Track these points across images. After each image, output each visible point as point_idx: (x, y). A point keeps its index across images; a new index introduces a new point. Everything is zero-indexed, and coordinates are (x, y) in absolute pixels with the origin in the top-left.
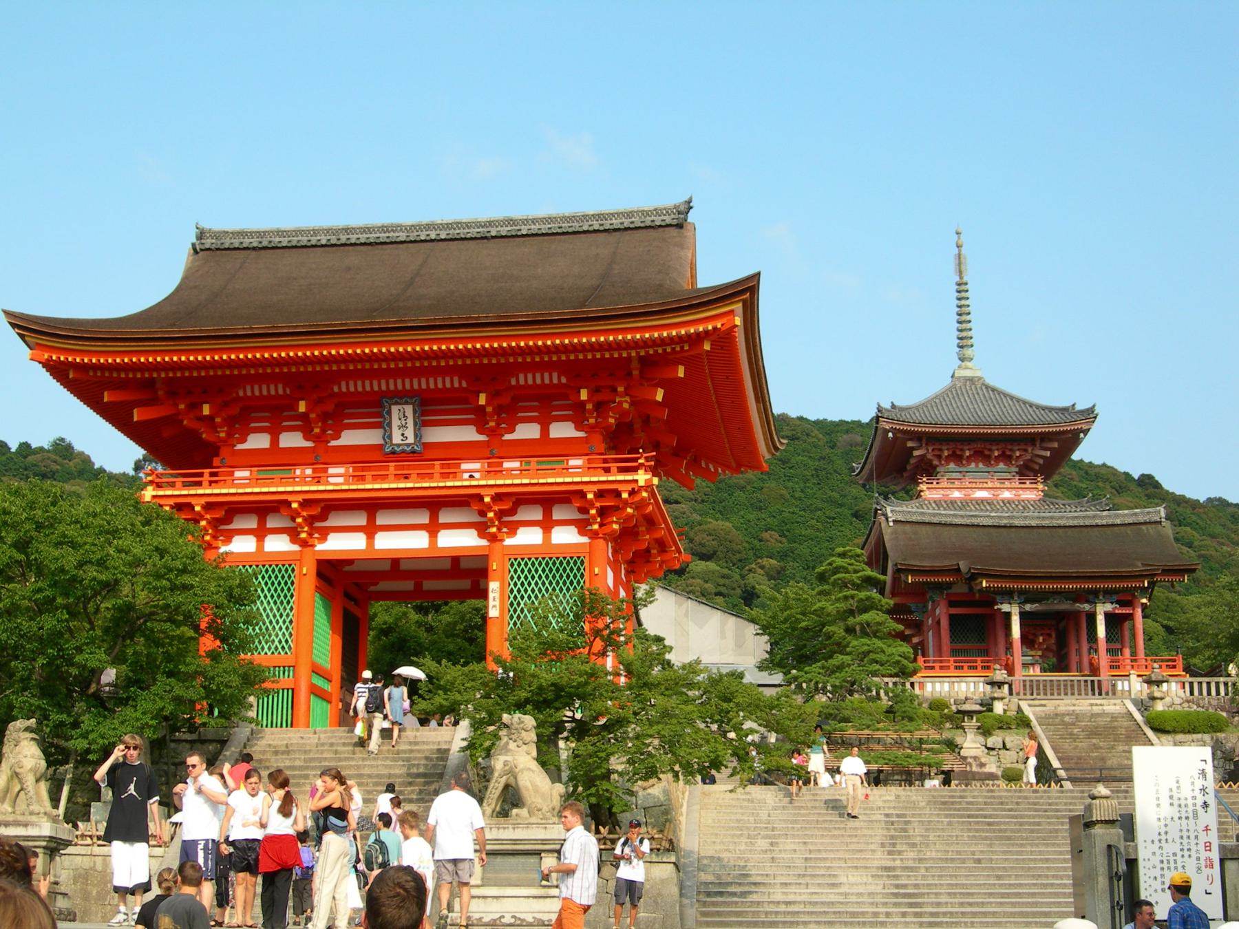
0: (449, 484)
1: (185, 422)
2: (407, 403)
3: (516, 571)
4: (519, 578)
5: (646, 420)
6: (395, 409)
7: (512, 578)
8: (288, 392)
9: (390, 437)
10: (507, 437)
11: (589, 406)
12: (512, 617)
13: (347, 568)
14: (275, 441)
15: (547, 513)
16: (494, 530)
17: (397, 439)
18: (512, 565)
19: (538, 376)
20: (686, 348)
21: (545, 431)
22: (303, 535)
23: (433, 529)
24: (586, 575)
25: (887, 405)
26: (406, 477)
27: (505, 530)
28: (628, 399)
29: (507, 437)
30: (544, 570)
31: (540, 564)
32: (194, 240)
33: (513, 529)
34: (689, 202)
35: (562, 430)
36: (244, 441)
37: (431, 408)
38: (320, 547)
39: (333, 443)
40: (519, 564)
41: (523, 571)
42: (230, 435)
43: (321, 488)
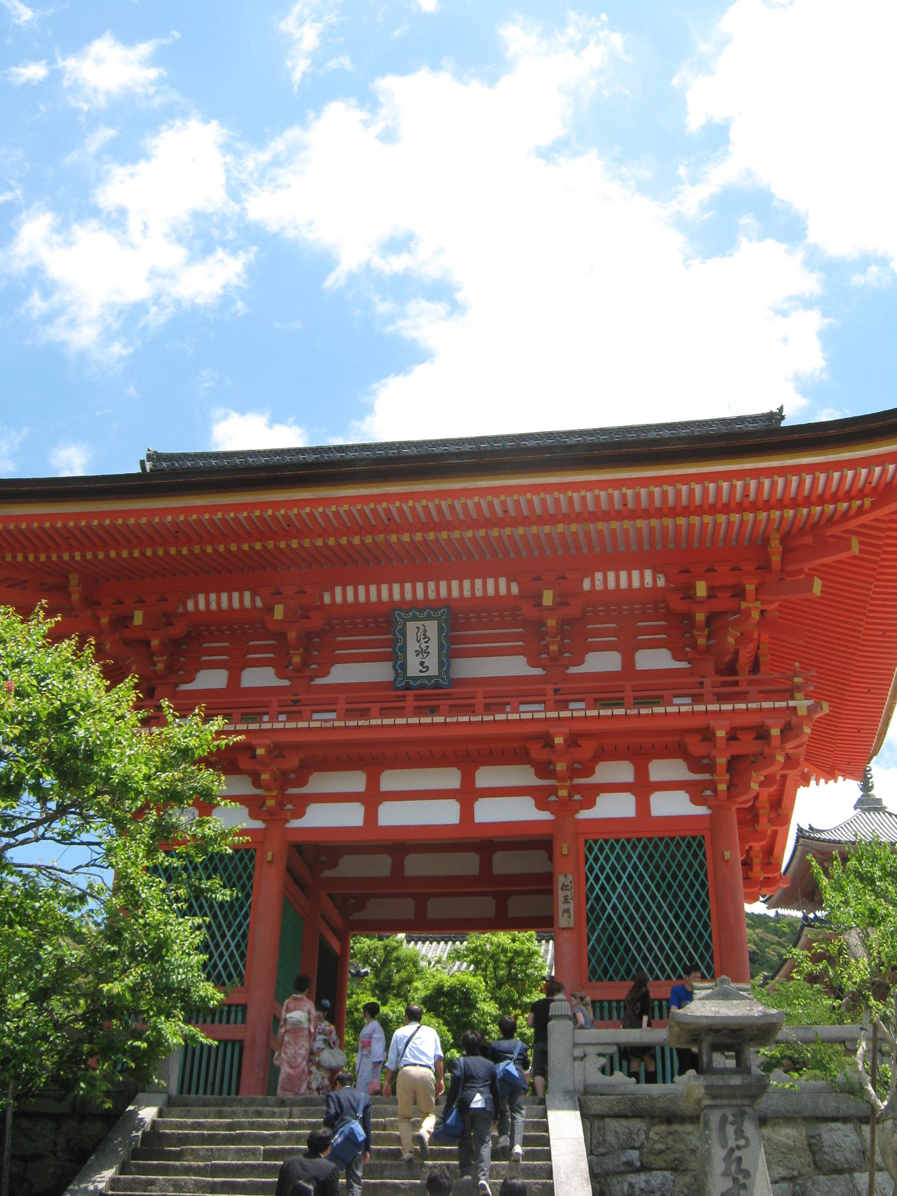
0: (500, 717)
1: (108, 646)
2: (429, 618)
3: (596, 859)
4: (602, 869)
5: (755, 668)
6: (411, 627)
7: (591, 869)
8: (259, 603)
9: (404, 666)
10: (573, 670)
11: (700, 617)
12: (592, 930)
13: (328, 873)
14: (235, 679)
15: (641, 772)
16: (563, 793)
17: (413, 669)
18: (590, 849)
19: (623, 575)
20: (867, 503)
21: (628, 662)
22: (270, 803)
23: (467, 795)
24: (708, 865)
25: (806, 828)
26: (433, 711)
27: (577, 797)
28: (758, 604)
29: (573, 670)
30: (640, 858)
31: (634, 848)
32: (145, 458)
33: (590, 795)
34: (781, 409)
35: (654, 660)
36: (192, 680)
37: (462, 627)
38: (294, 824)
39: (319, 681)
40: (601, 849)
41: (607, 858)
42: (171, 668)
43: (303, 725)
